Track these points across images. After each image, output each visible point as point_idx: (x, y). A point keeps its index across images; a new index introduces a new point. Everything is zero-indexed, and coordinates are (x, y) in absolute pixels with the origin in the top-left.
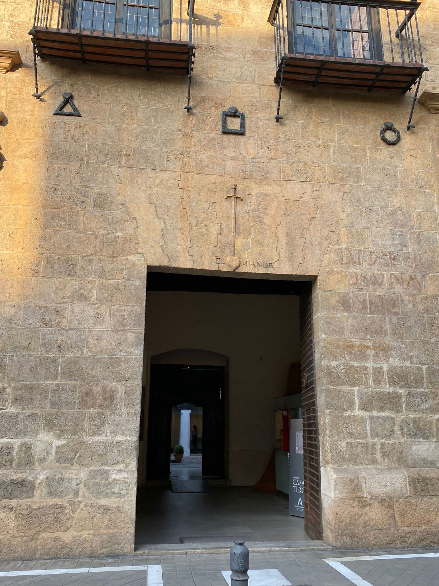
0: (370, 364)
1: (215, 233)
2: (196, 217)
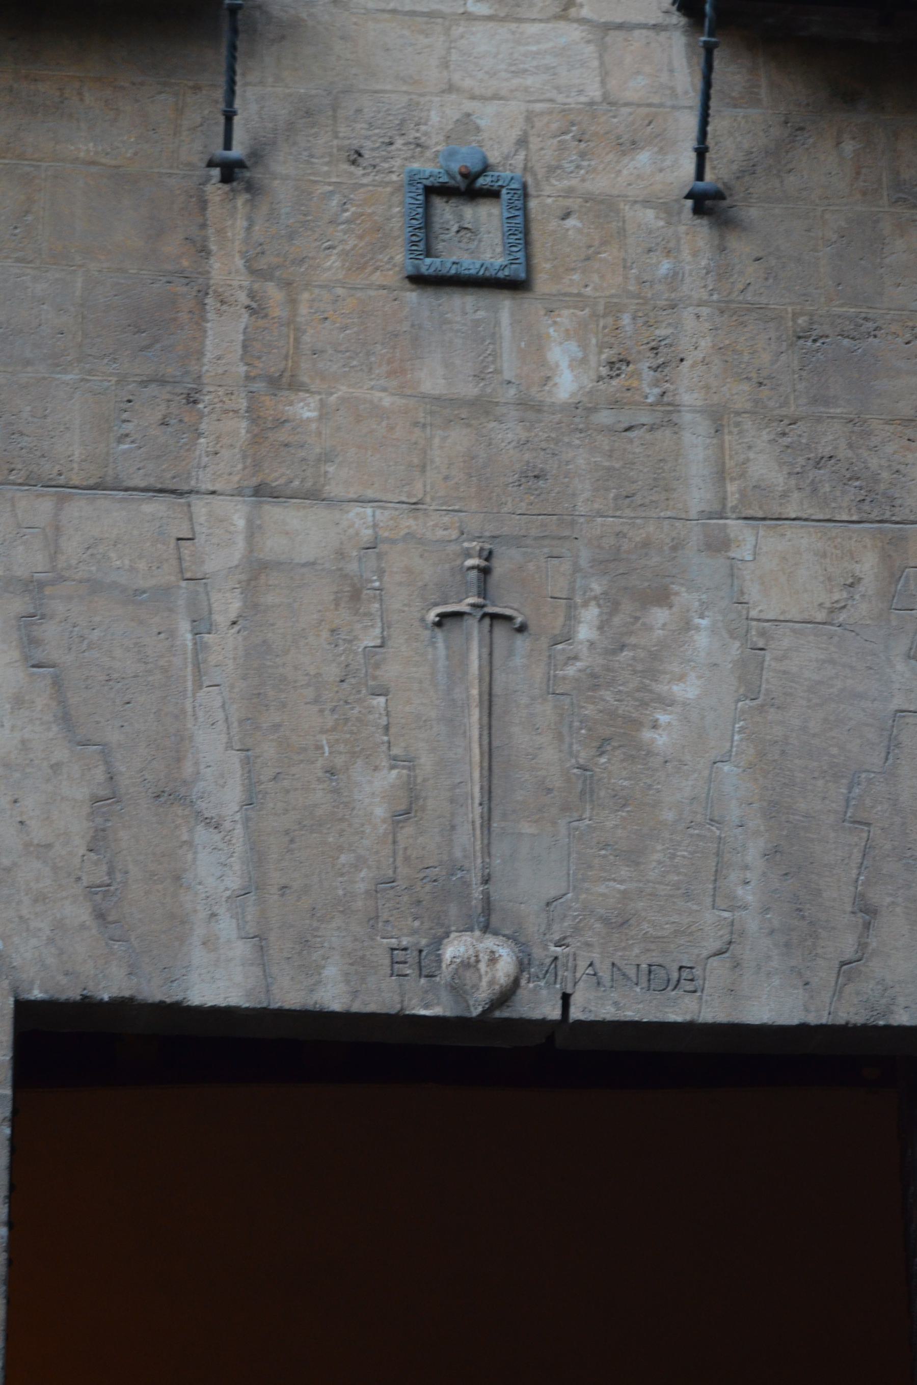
1: (380, 811)
2: (276, 727)
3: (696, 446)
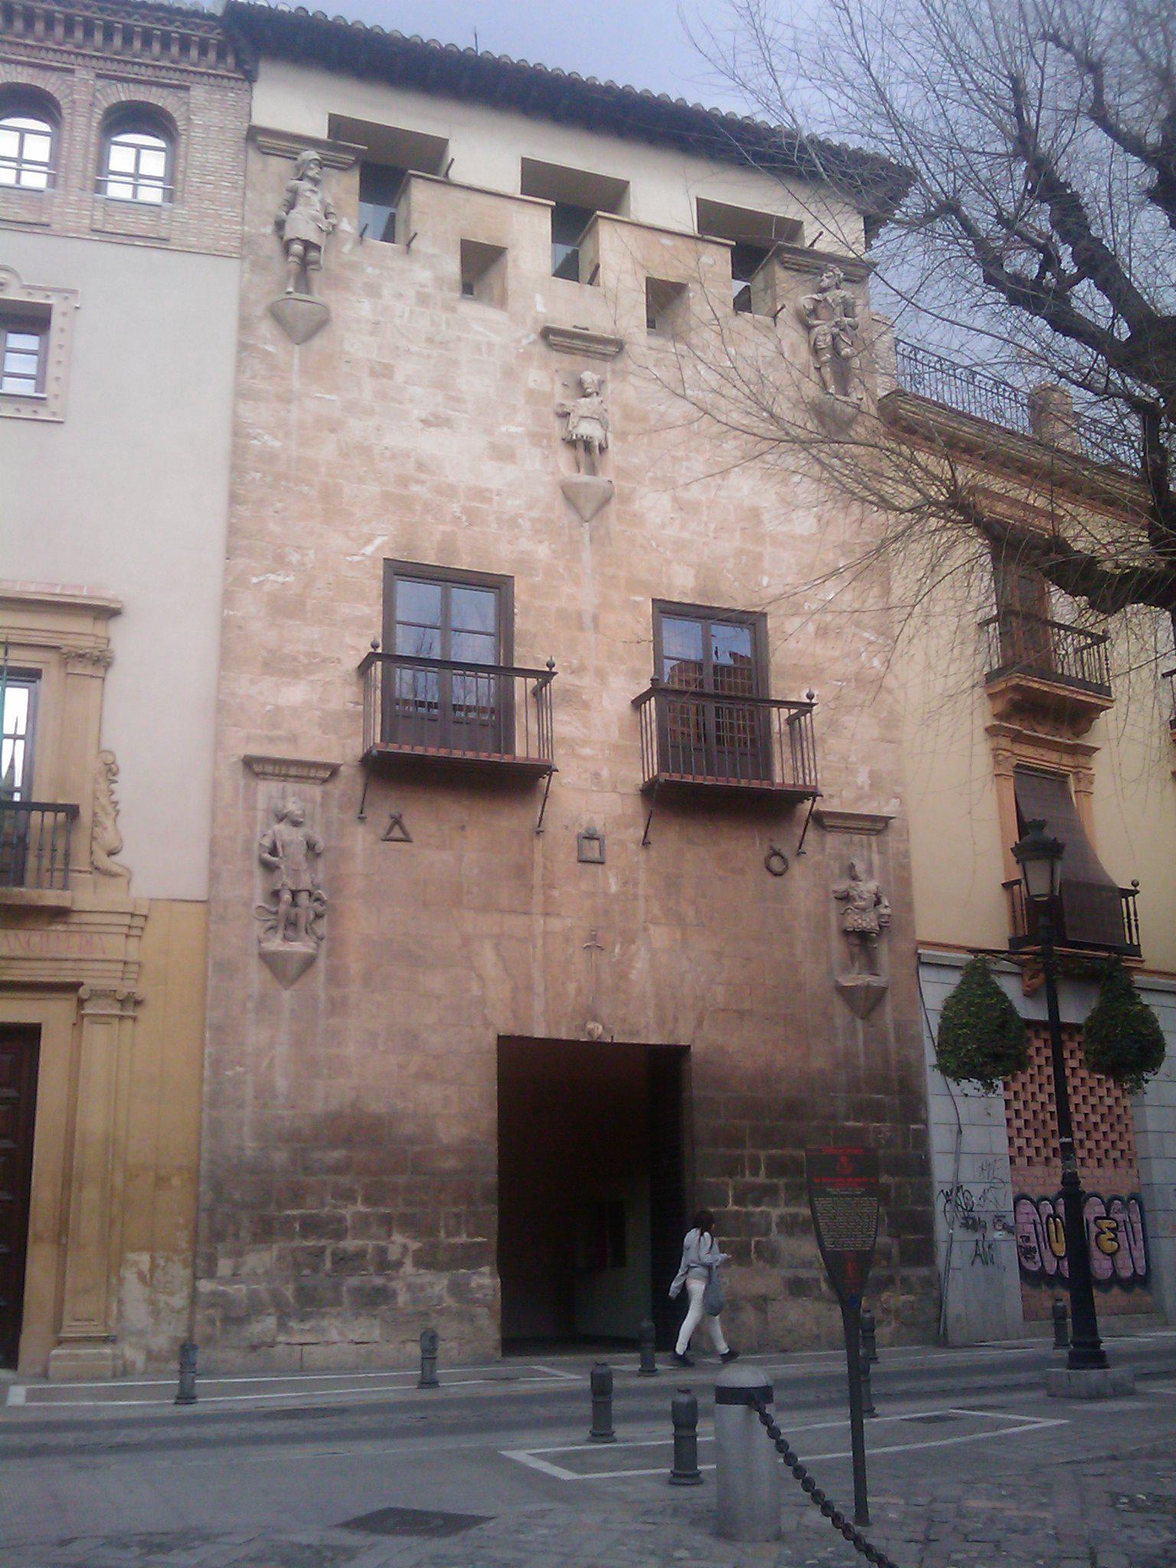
0: (748, 1152)
3: (641, 903)
